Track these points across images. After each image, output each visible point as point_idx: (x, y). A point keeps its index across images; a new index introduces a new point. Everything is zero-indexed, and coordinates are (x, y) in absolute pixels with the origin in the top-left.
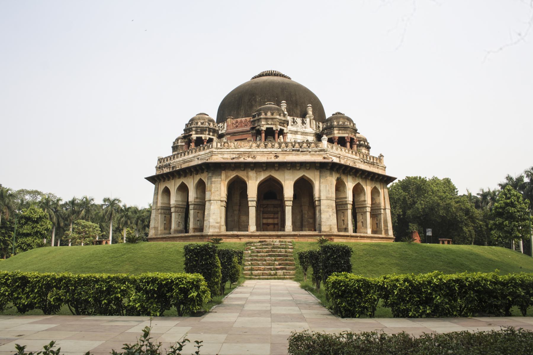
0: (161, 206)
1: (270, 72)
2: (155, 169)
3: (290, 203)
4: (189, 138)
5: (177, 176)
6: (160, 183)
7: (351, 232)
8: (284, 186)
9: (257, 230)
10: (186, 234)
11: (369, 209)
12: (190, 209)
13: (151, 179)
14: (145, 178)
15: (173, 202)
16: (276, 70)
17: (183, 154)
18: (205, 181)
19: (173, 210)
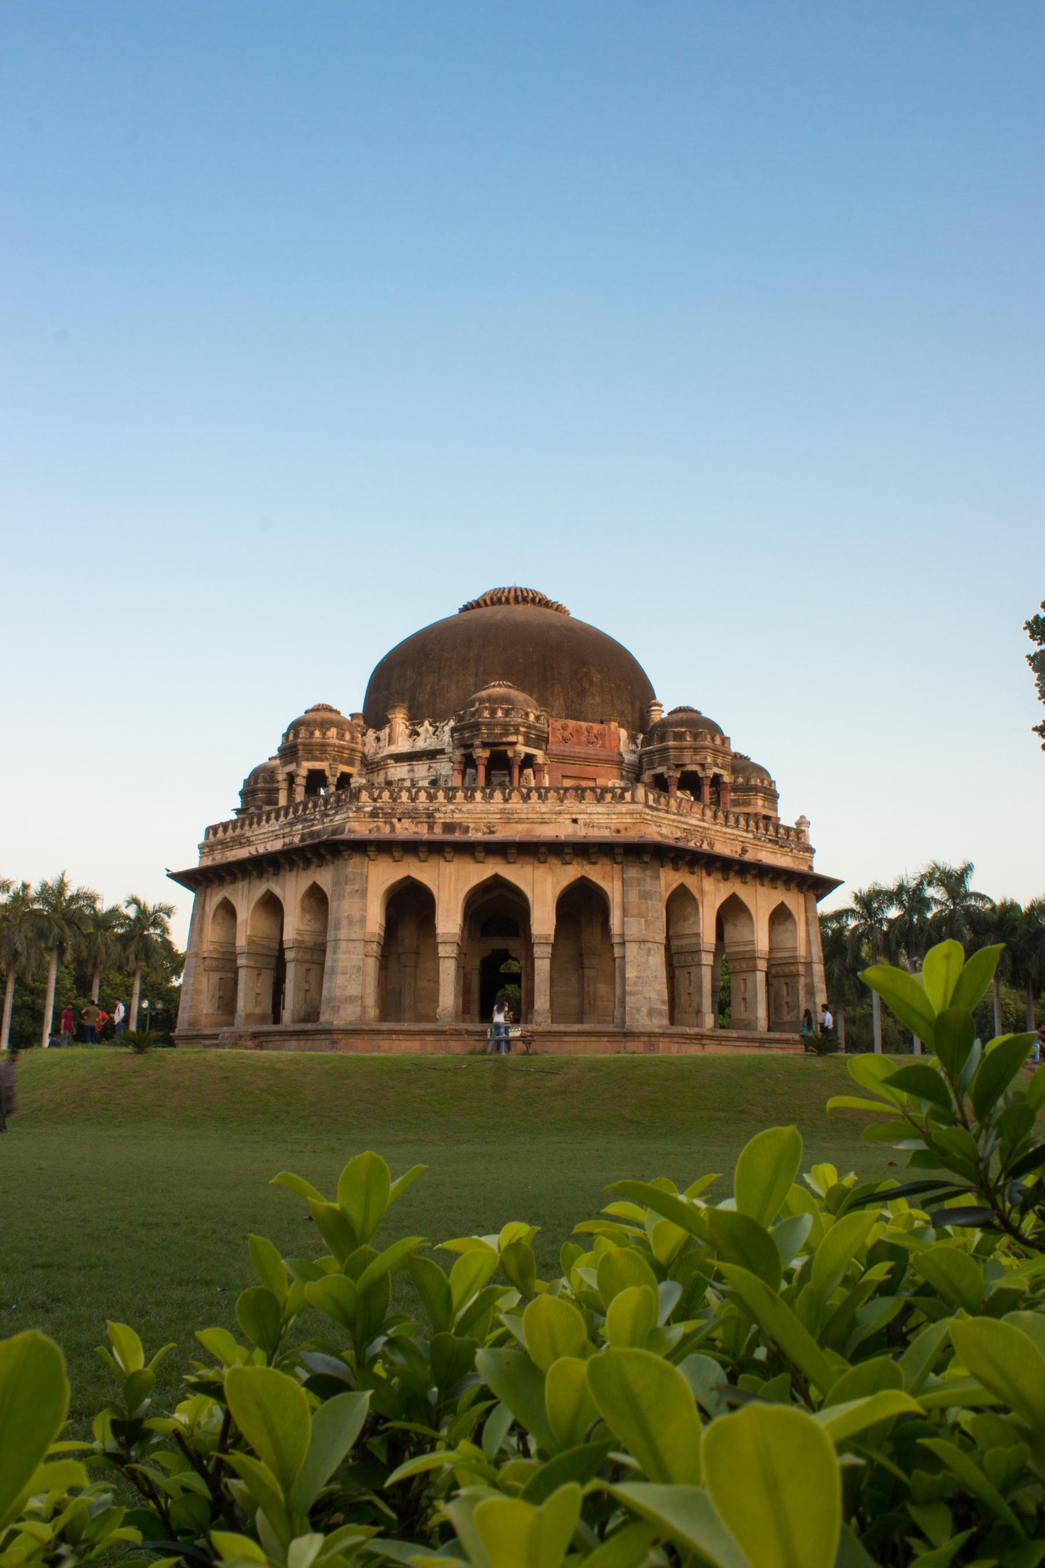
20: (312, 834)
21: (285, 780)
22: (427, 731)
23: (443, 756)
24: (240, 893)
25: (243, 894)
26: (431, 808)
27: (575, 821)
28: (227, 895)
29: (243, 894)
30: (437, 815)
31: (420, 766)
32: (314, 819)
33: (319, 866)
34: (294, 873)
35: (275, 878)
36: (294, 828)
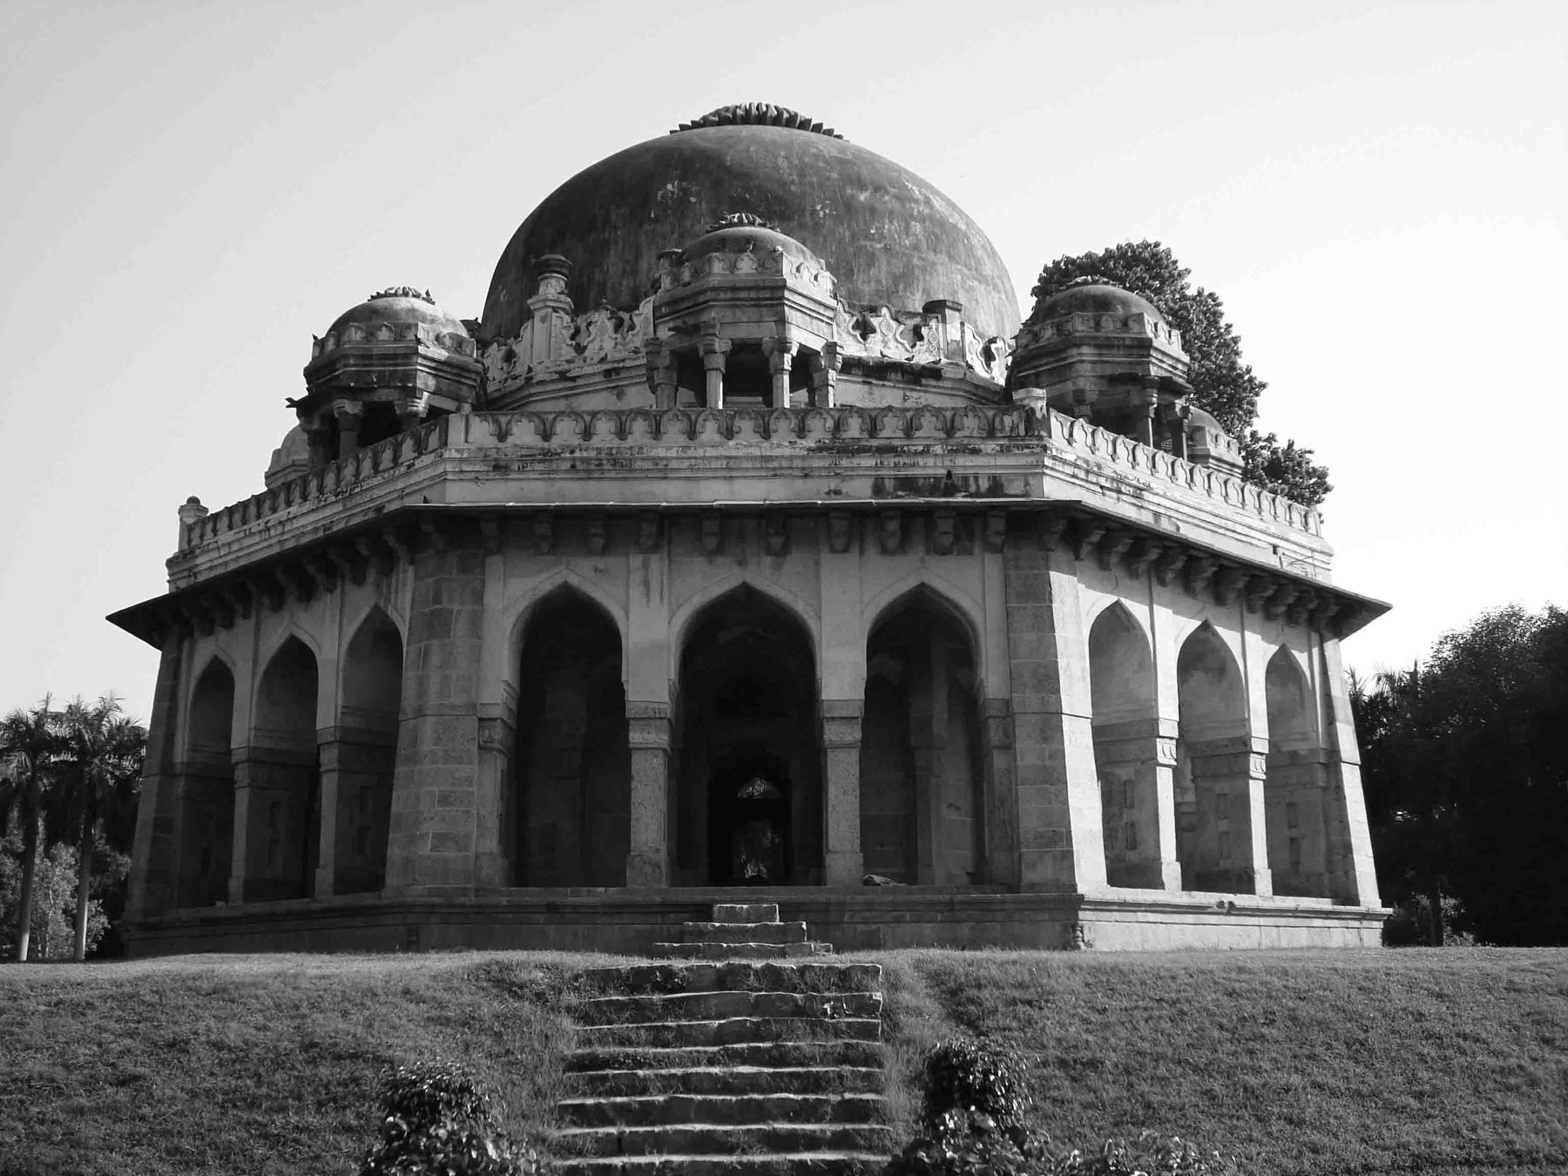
0: (188, 764)
1: (754, 111)
2: (164, 574)
3: (854, 734)
4: (324, 409)
5: (266, 601)
6: (186, 644)
7: (1172, 888)
8: (816, 639)
9: (677, 880)
10: (296, 904)
11: (1257, 766)
12: (322, 770)
13: (134, 620)
14: (111, 618)
15: (243, 729)
16: (781, 106)
17: (297, 493)
18: (402, 613)
19: (242, 775)
20: (907, 484)
21: (723, 353)
22: (889, 328)
23: (934, 383)
24: (636, 578)
25: (646, 583)
26: (1142, 481)
27: (1275, 548)
28: (574, 580)
29: (646, 583)
30: (1146, 495)
31: (887, 391)
32: (926, 452)
33: (959, 554)
34: (853, 555)
35: (768, 560)
36: (844, 462)
